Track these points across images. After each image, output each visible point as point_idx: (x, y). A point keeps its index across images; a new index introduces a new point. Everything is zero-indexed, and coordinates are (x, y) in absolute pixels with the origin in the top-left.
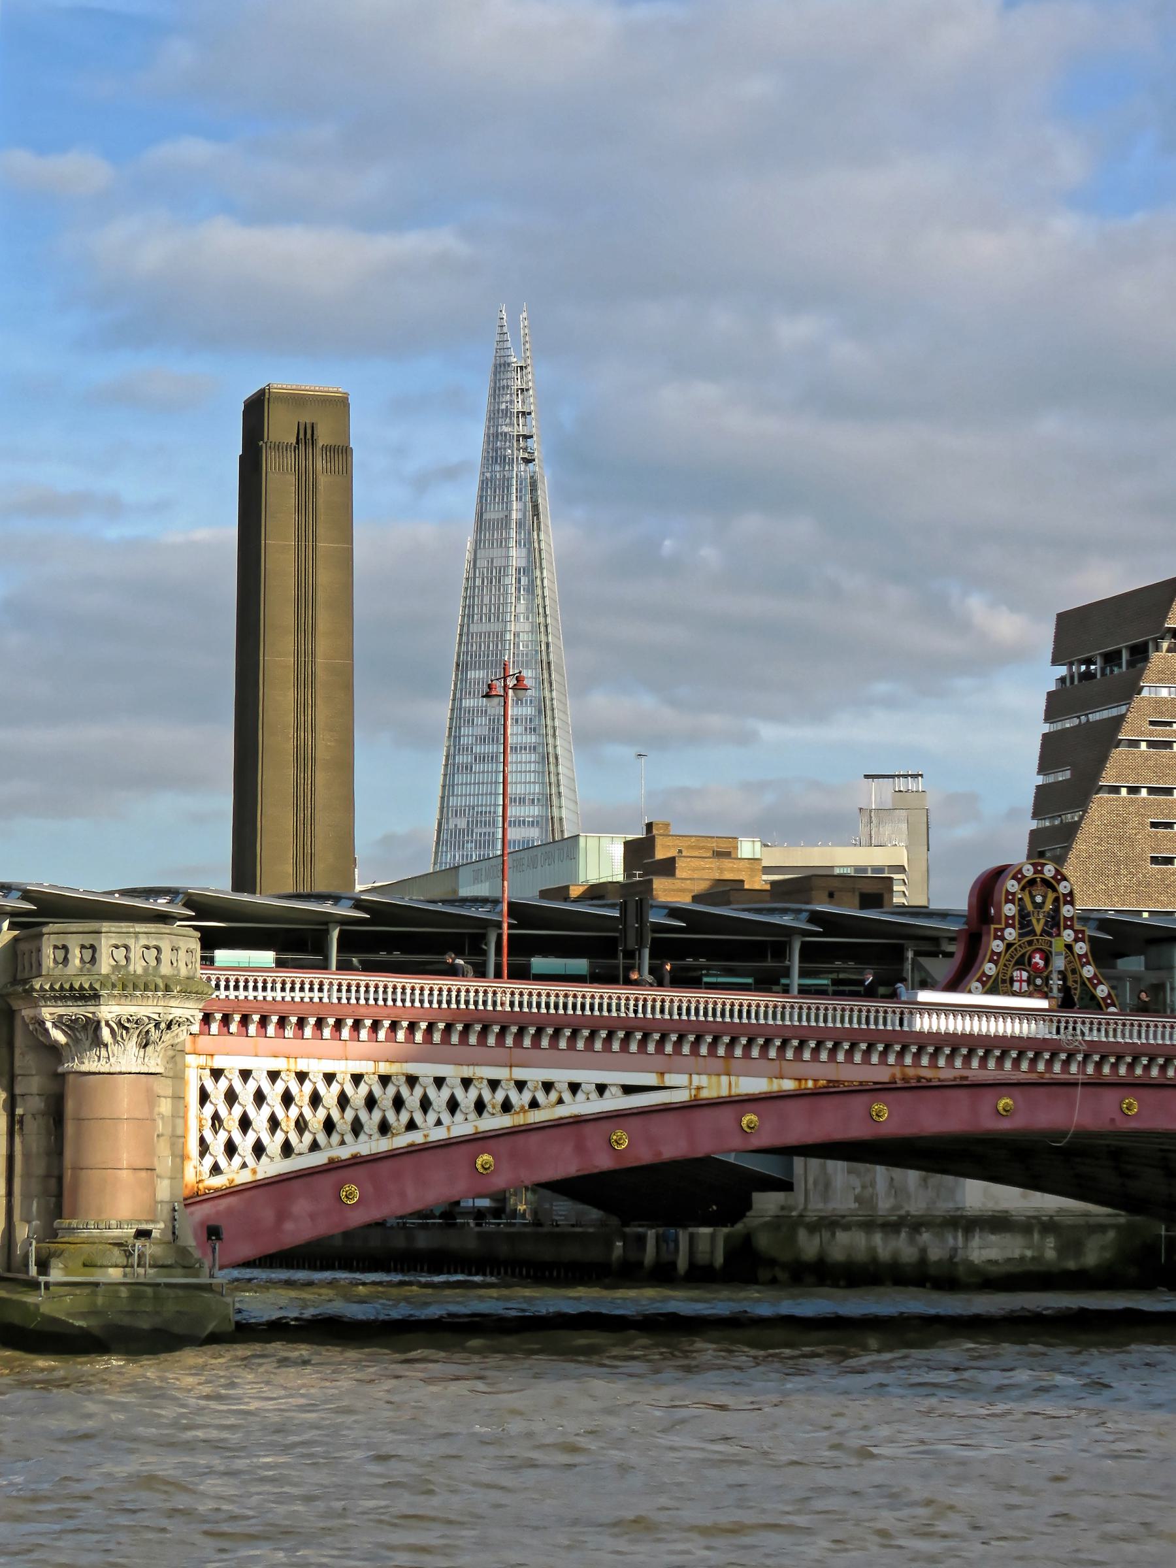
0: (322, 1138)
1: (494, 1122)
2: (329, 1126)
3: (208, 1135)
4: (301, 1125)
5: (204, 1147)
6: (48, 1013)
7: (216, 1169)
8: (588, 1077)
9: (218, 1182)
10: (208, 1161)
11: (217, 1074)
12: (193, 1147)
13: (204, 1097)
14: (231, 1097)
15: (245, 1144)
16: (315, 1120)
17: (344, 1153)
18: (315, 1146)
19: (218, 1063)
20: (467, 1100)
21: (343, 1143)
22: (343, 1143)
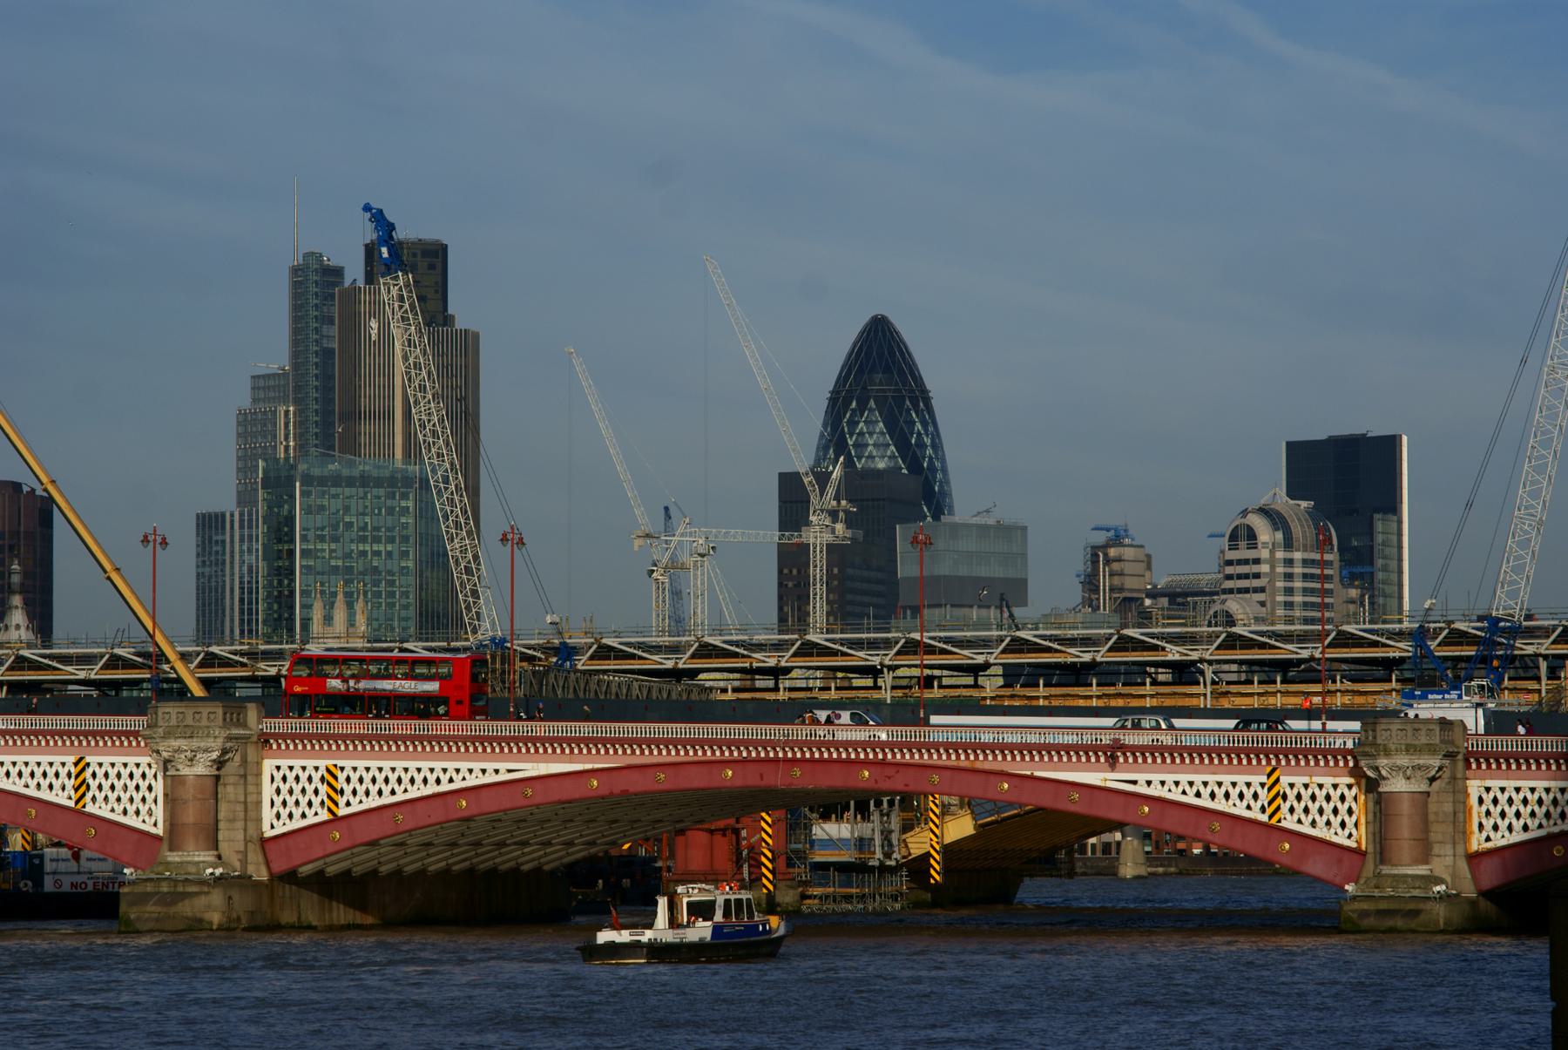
0: (1544, 822)
2: (1548, 815)
3: (1484, 821)
4: (1518, 815)
5: (1481, 826)
7: (1488, 839)
9: (1490, 845)
10: (1484, 835)
11: (1488, 790)
12: (1475, 827)
13: (1481, 801)
14: (1495, 801)
15: (1503, 825)
16: (1540, 812)
17: (1556, 830)
18: (1540, 826)
19: (1488, 783)
21: (1555, 824)
22: (1555, 824)
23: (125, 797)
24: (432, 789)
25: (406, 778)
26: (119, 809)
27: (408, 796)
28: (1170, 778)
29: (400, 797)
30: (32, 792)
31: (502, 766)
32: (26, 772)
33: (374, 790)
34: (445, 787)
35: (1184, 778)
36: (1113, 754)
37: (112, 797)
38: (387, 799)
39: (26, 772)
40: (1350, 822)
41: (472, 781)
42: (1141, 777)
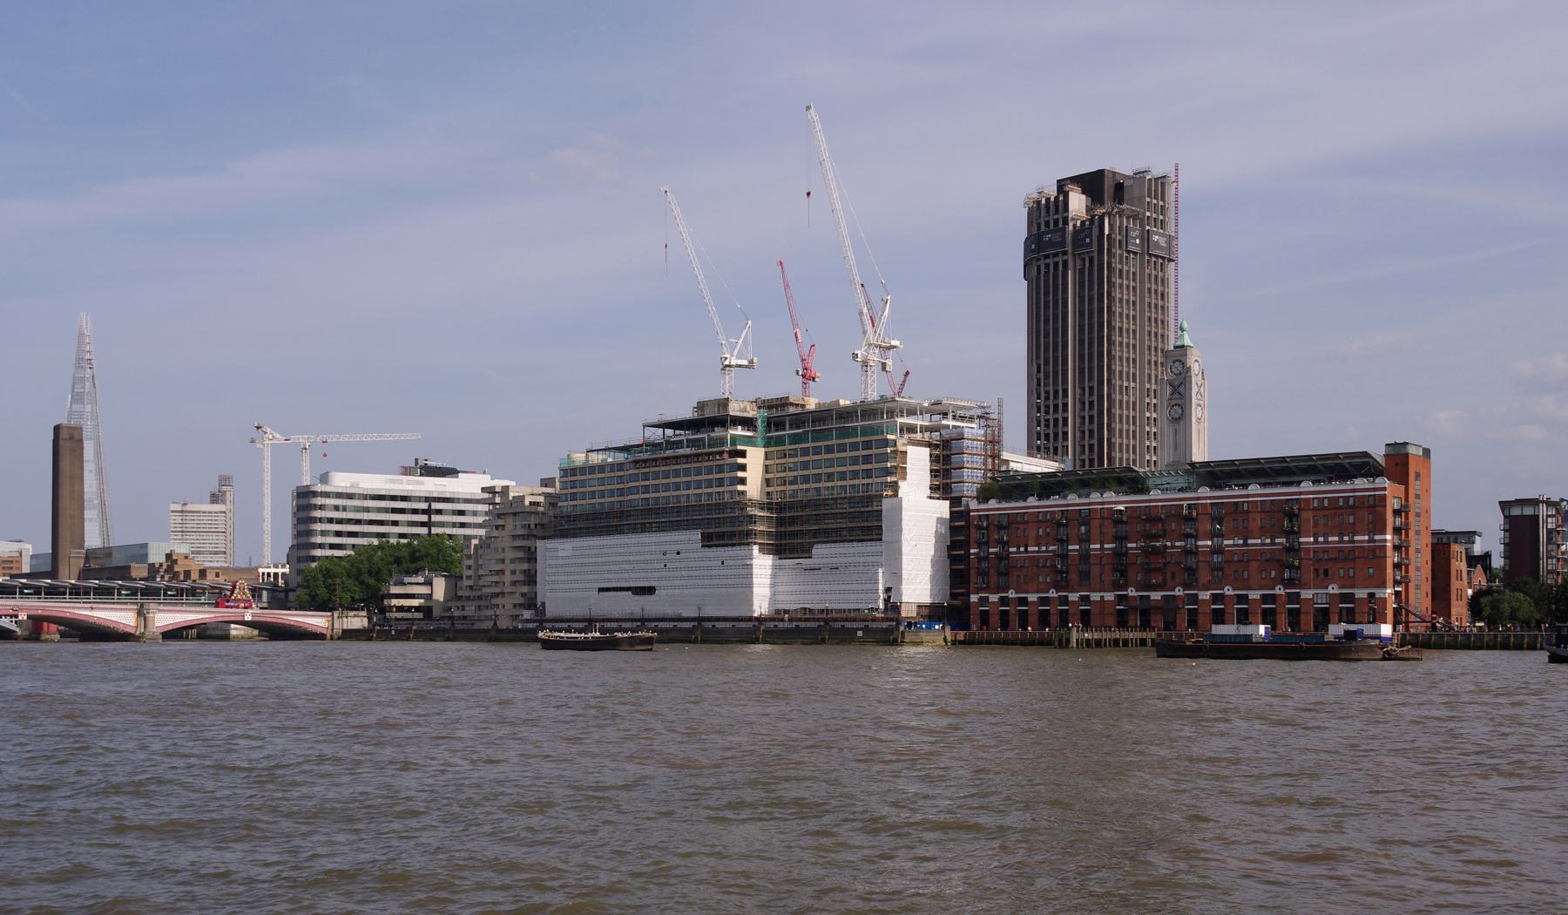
36: (92, 608)
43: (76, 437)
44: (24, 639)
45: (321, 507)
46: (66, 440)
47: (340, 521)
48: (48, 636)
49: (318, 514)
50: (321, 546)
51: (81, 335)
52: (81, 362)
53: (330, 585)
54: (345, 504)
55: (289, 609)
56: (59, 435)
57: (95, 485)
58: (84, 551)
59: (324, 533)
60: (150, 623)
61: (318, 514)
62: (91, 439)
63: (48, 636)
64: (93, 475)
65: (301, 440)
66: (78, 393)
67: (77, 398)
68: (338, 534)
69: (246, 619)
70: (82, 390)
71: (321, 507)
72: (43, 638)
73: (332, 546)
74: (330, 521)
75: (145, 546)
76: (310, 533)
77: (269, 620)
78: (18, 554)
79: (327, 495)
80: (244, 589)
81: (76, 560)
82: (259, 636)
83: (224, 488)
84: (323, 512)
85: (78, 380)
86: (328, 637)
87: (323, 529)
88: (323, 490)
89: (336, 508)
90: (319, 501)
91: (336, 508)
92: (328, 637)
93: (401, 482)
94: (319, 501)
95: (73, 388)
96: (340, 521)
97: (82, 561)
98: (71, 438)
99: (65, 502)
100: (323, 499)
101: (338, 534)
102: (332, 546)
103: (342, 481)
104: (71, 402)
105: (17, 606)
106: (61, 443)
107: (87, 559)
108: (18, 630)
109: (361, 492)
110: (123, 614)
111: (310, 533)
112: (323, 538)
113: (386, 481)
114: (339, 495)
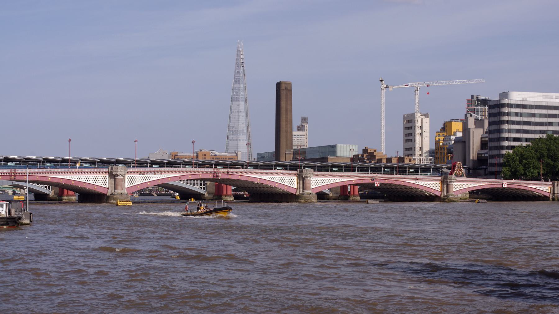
1: (468, 187)
6: (448, 181)
8: (473, 184)
20: (466, 186)
23: (291, 183)
24: (333, 182)
25: (330, 181)
26: (290, 184)
27: (330, 183)
28: (421, 182)
29: (329, 183)
30: (277, 182)
31: (342, 179)
32: (276, 179)
33: (325, 182)
34: (335, 182)
35: (422, 182)
36: (416, 179)
37: (289, 183)
38: (327, 184)
39: (276, 179)
40: (440, 188)
41: (338, 181)
42: (418, 182)
43: (289, 89)
44: (334, 199)
45: (509, 114)
46: (283, 90)
47: (519, 123)
48: (354, 198)
49: (506, 118)
50: (508, 139)
51: (239, 51)
52: (239, 64)
53: (525, 164)
54: (521, 112)
55: (527, 180)
56: (280, 88)
57: (245, 123)
58: (293, 150)
59: (510, 131)
60: (451, 189)
61: (506, 118)
62: (243, 101)
63: (354, 198)
64: (244, 118)
65: (414, 85)
66: (237, 79)
67: (237, 81)
68: (518, 131)
69: (504, 186)
70: (239, 77)
71: (509, 114)
72: (352, 199)
73: (515, 140)
74: (513, 123)
75: (334, 147)
76: (500, 131)
77: (516, 187)
78: (235, 155)
79: (511, 106)
80: (460, 168)
81: (289, 155)
82: (470, 197)
83: (304, 124)
84: (510, 117)
85: (237, 73)
86: (551, 199)
87: (510, 128)
88: (510, 103)
89: (517, 114)
90: (506, 110)
91: (517, 114)
92: (551, 199)
93: (552, 97)
94: (506, 110)
95: (235, 77)
96: (519, 123)
97: (292, 156)
98: (286, 88)
99: (283, 124)
100: (510, 109)
101: (518, 131)
102: (515, 140)
103: (516, 97)
104: (234, 83)
105: (374, 177)
106: (282, 92)
107: (294, 154)
108: (329, 193)
109: (531, 104)
110: (434, 182)
111: (500, 131)
112: (510, 134)
113: (543, 97)
114: (518, 106)
